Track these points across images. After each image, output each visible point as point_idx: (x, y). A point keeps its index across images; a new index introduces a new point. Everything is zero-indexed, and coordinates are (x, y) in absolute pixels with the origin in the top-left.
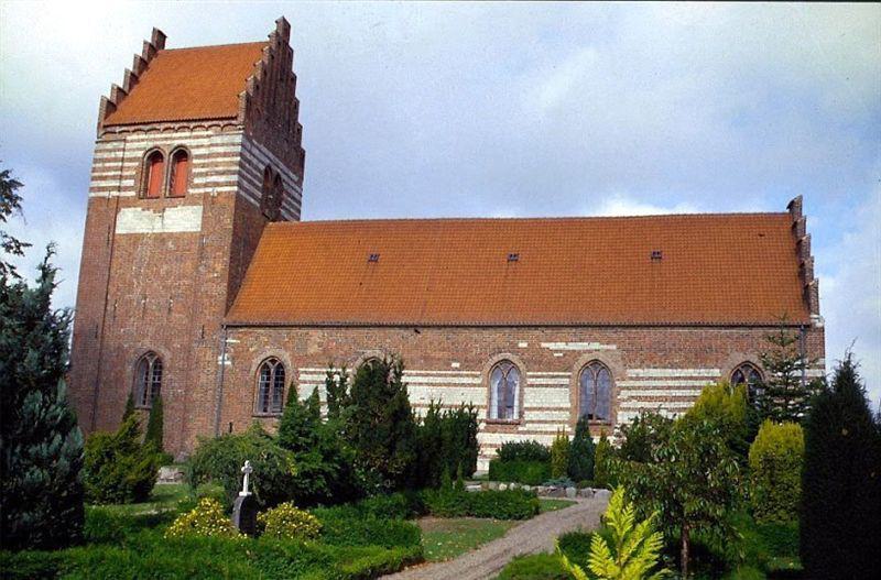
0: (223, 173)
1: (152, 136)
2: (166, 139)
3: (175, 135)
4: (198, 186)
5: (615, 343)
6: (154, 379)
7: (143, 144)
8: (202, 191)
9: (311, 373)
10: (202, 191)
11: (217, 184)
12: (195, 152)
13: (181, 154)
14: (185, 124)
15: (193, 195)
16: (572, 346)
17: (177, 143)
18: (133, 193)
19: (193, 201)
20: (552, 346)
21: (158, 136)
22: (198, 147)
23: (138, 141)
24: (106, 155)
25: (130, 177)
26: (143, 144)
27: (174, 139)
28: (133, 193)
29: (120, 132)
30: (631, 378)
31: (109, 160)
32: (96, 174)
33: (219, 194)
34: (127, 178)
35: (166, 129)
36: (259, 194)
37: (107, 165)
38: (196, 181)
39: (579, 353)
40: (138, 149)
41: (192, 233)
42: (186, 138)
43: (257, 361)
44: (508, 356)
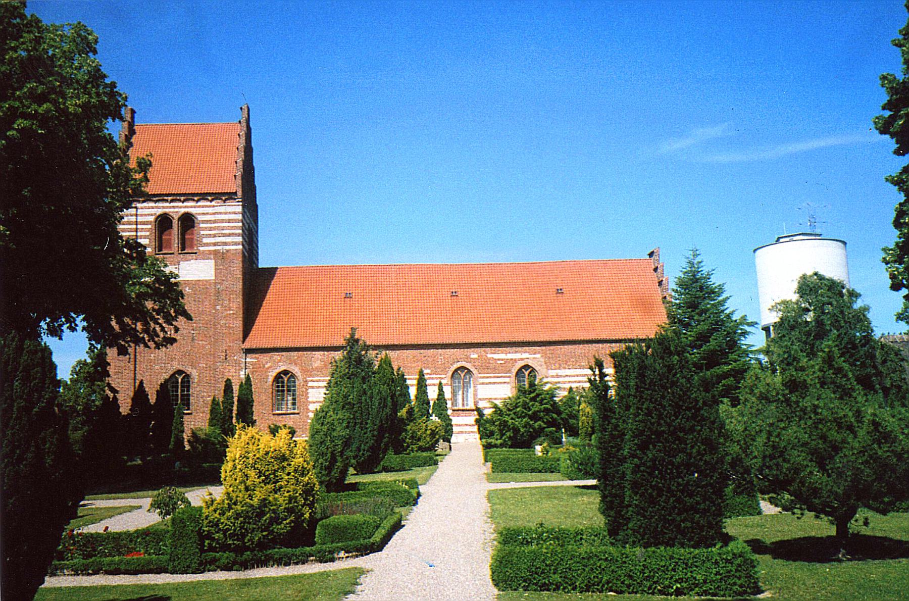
0: (229, 235)
2: (174, 207)
4: (207, 245)
5: (539, 353)
9: (317, 381)
10: (212, 248)
11: (225, 244)
12: (200, 218)
15: (204, 251)
16: (510, 356)
17: (183, 211)
19: (205, 256)
20: (496, 356)
21: (167, 204)
22: (204, 214)
25: (145, 237)
27: (181, 207)
30: (553, 377)
33: (228, 251)
35: (172, 201)
38: (205, 240)
39: (515, 361)
40: (152, 215)
42: (191, 207)
43: (273, 374)
44: (464, 364)
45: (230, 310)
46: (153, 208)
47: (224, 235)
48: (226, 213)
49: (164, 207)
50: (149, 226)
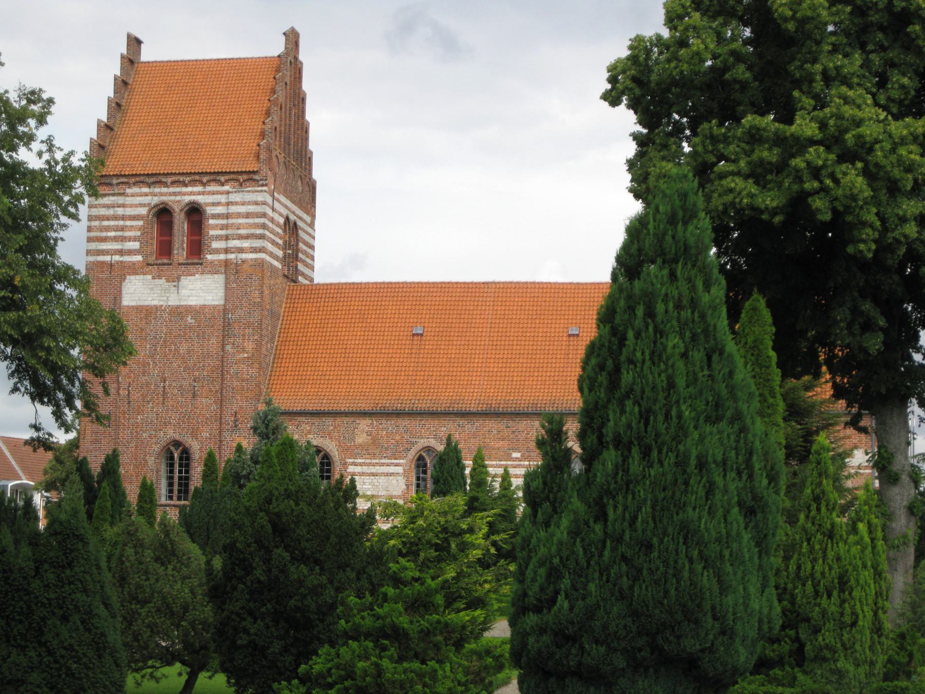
0: (247, 237)
1: (157, 190)
2: (175, 194)
3: (184, 189)
4: (217, 251)
6: (180, 472)
7: (147, 200)
8: (222, 257)
9: (361, 465)
10: (222, 257)
11: (241, 250)
12: (210, 210)
13: (195, 212)
14: (197, 177)
15: (212, 262)
17: (187, 199)
18: (139, 258)
19: (213, 269)
21: (164, 190)
23: (141, 195)
24: (103, 212)
25: (135, 239)
26: (147, 200)
27: (184, 194)
28: (139, 258)
29: (118, 184)
31: (108, 218)
32: (93, 234)
33: (243, 261)
34: (130, 239)
35: (173, 183)
36: (280, 253)
37: (106, 223)
38: (215, 245)
40: (141, 205)
41: (215, 307)
42: (199, 193)
45: (244, 351)
46: (146, 195)
47: (241, 237)
48: (243, 204)
49: (161, 194)
50: (141, 223)
